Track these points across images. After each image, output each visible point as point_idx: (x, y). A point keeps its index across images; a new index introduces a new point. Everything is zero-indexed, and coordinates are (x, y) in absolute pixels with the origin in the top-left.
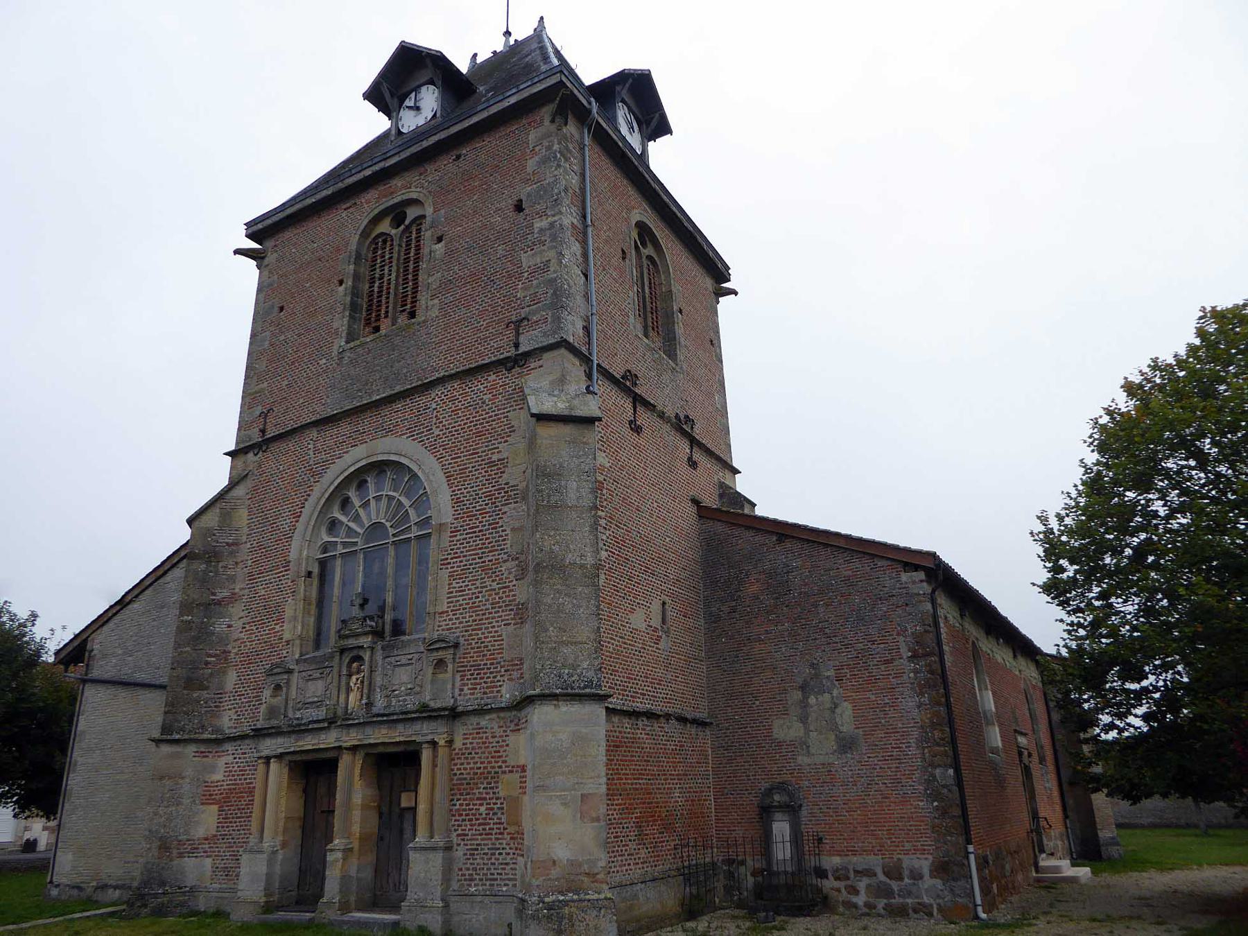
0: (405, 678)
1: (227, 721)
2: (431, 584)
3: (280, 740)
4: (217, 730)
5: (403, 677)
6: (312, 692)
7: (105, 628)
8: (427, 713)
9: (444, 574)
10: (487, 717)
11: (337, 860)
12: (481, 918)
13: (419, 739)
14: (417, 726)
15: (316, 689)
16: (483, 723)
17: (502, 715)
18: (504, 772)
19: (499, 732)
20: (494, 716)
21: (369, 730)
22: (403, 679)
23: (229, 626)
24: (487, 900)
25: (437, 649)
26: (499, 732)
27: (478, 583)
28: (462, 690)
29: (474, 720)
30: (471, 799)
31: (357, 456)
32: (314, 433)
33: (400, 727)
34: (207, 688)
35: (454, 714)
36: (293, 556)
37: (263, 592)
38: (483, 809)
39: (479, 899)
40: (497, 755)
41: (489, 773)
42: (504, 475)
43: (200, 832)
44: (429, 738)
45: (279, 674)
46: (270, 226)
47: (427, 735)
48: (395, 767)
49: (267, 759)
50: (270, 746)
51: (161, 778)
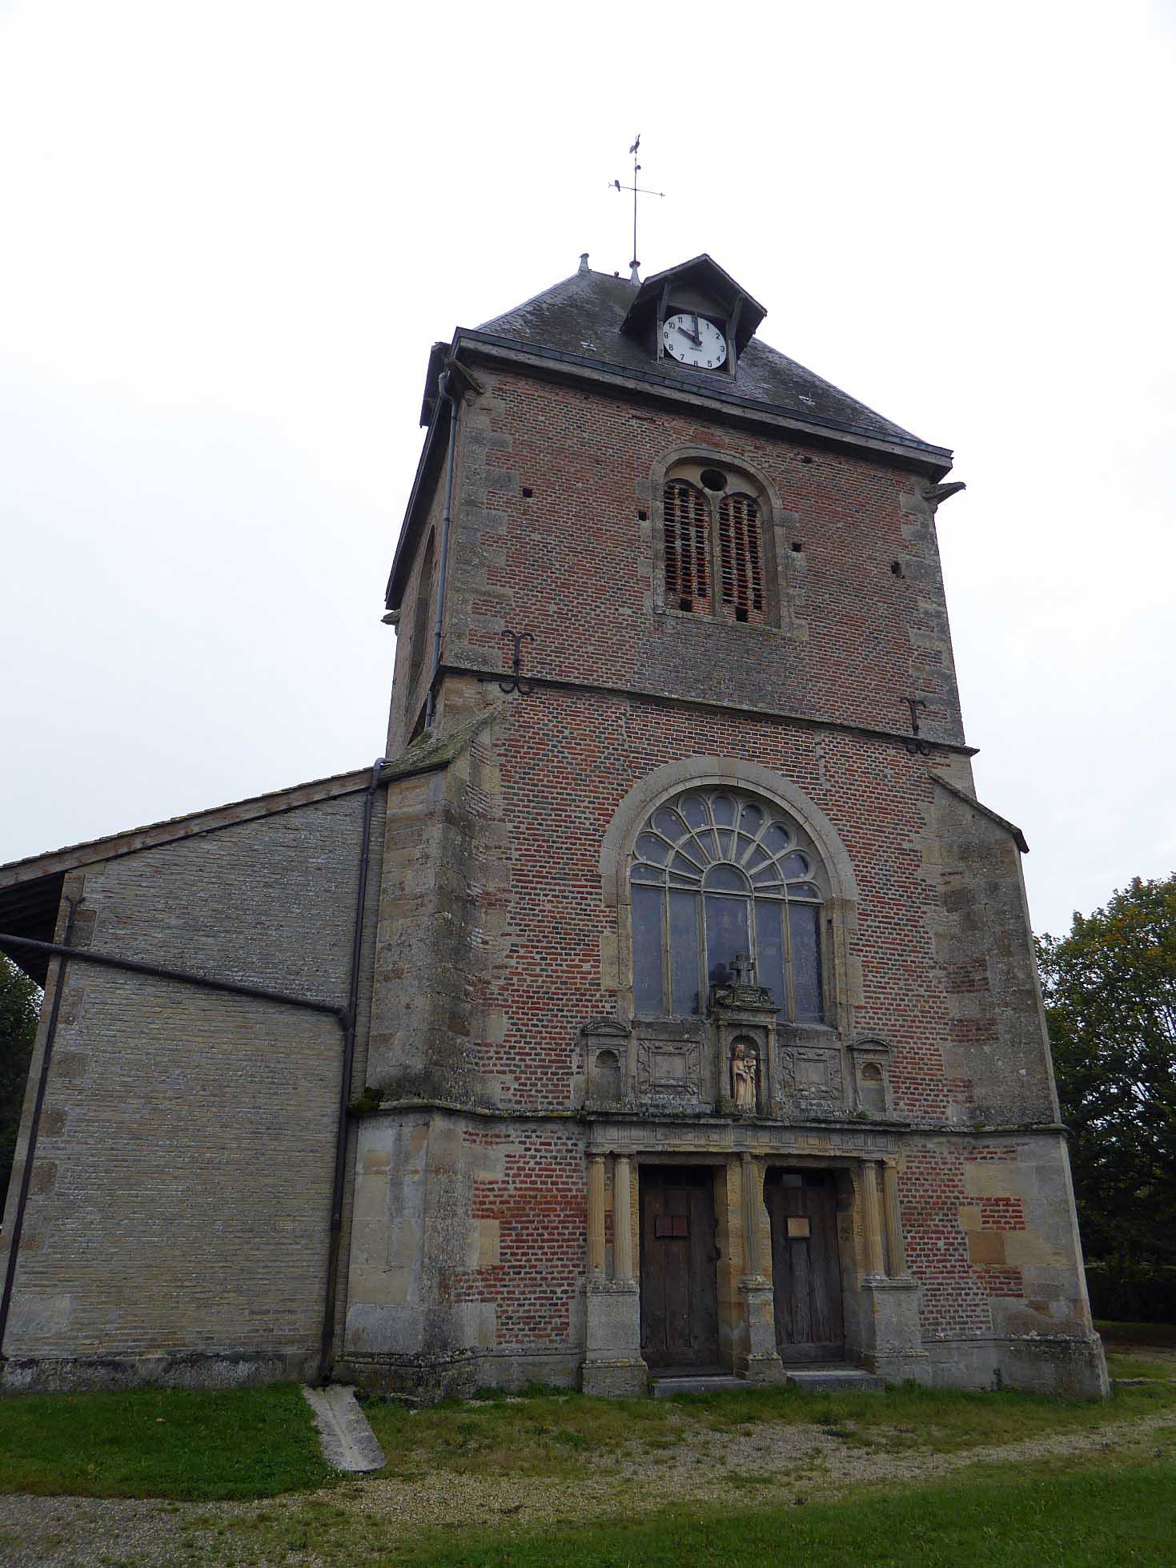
0: (815, 1078)
1: (499, 1089)
2: (839, 970)
3: (636, 1133)
4: (487, 1103)
5: (811, 1076)
6: (671, 1073)
7: (114, 867)
8: (856, 1126)
9: (857, 960)
10: (936, 1140)
11: (766, 1304)
12: (961, 1366)
13: (865, 1156)
14: (860, 1140)
15: (671, 1068)
16: (930, 1146)
17: (954, 1139)
18: (962, 1204)
19: (950, 1159)
20: (943, 1139)
21: (788, 1137)
22: (813, 1079)
23: (485, 942)
24: (964, 1346)
25: (867, 1051)
26: (950, 1159)
27: (902, 983)
28: (897, 1104)
29: (919, 1141)
30: (925, 1232)
31: (704, 768)
32: (626, 706)
33: (836, 1139)
34: (467, 1034)
35: (897, 1131)
36: (605, 868)
37: (548, 907)
38: (941, 1244)
39: (954, 1345)
40: (951, 1184)
41: (944, 1203)
42: (919, 870)
43: (474, 1262)
44: (877, 1156)
45: (604, 1036)
46: (616, 386)
47: (872, 1152)
48: (814, 1190)
49: (613, 1157)
50: (609, 1139)
51: (437, 1172)
